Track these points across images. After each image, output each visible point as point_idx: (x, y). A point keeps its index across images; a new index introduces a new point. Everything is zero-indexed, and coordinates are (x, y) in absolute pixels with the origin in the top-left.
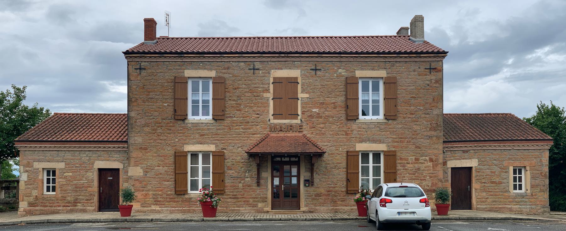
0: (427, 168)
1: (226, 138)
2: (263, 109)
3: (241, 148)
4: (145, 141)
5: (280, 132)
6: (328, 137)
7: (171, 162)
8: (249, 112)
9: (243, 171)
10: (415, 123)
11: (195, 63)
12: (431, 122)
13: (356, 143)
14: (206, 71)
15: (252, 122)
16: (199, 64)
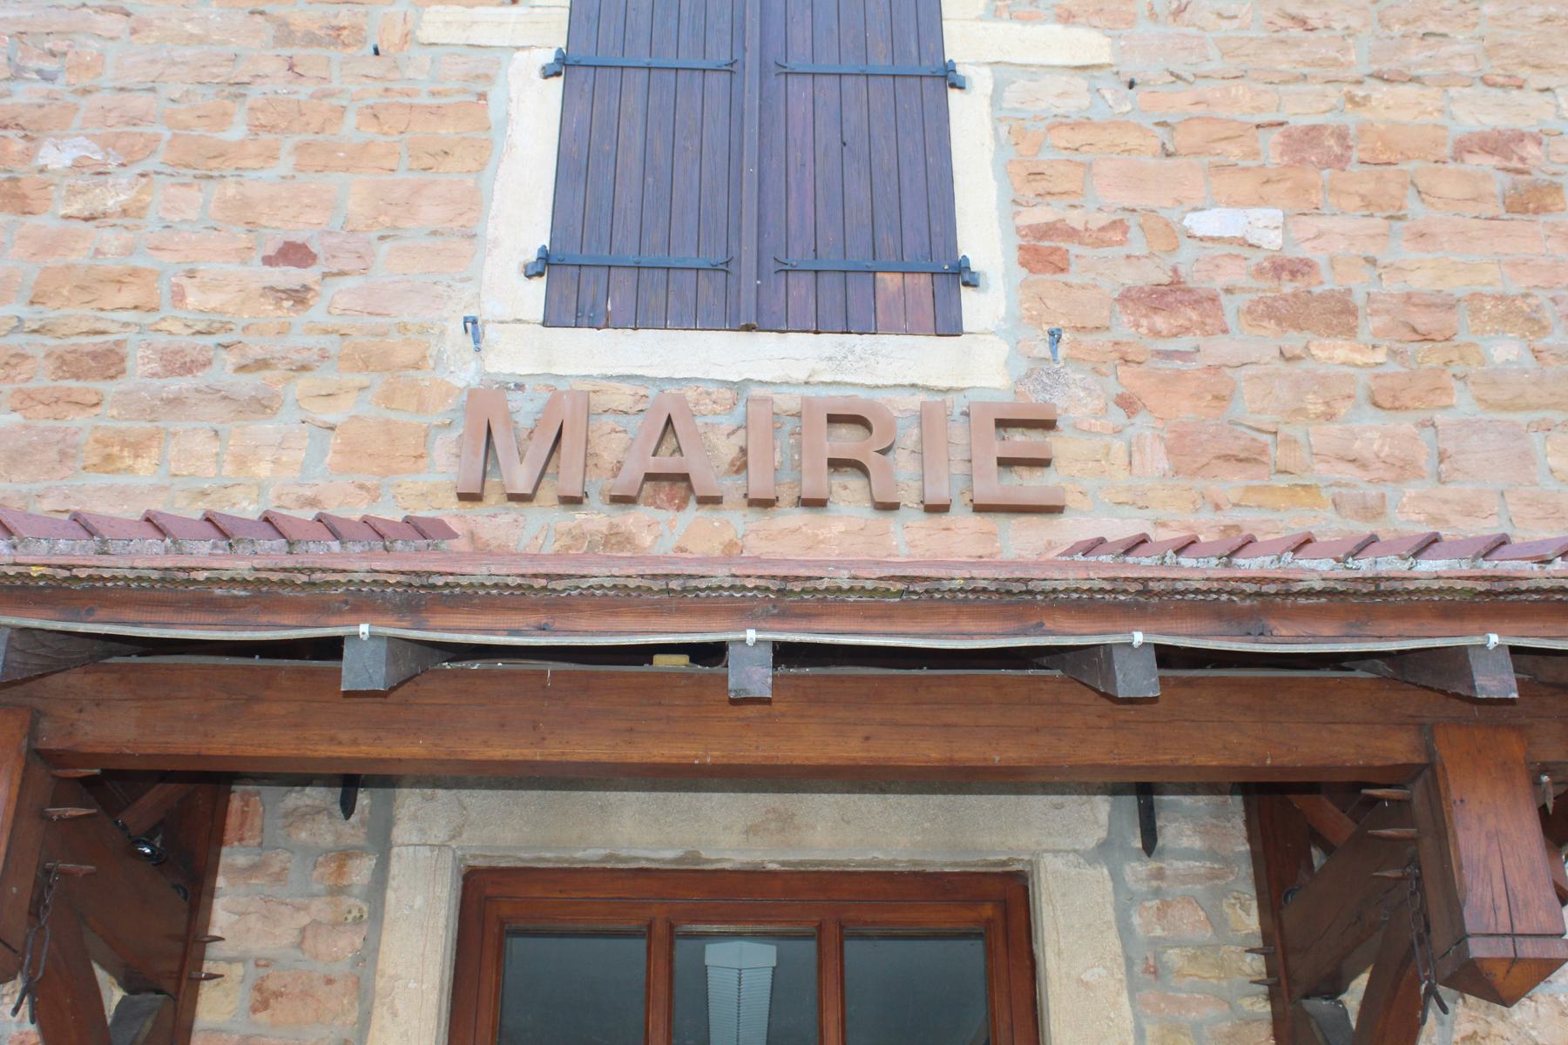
15: (179, 364)
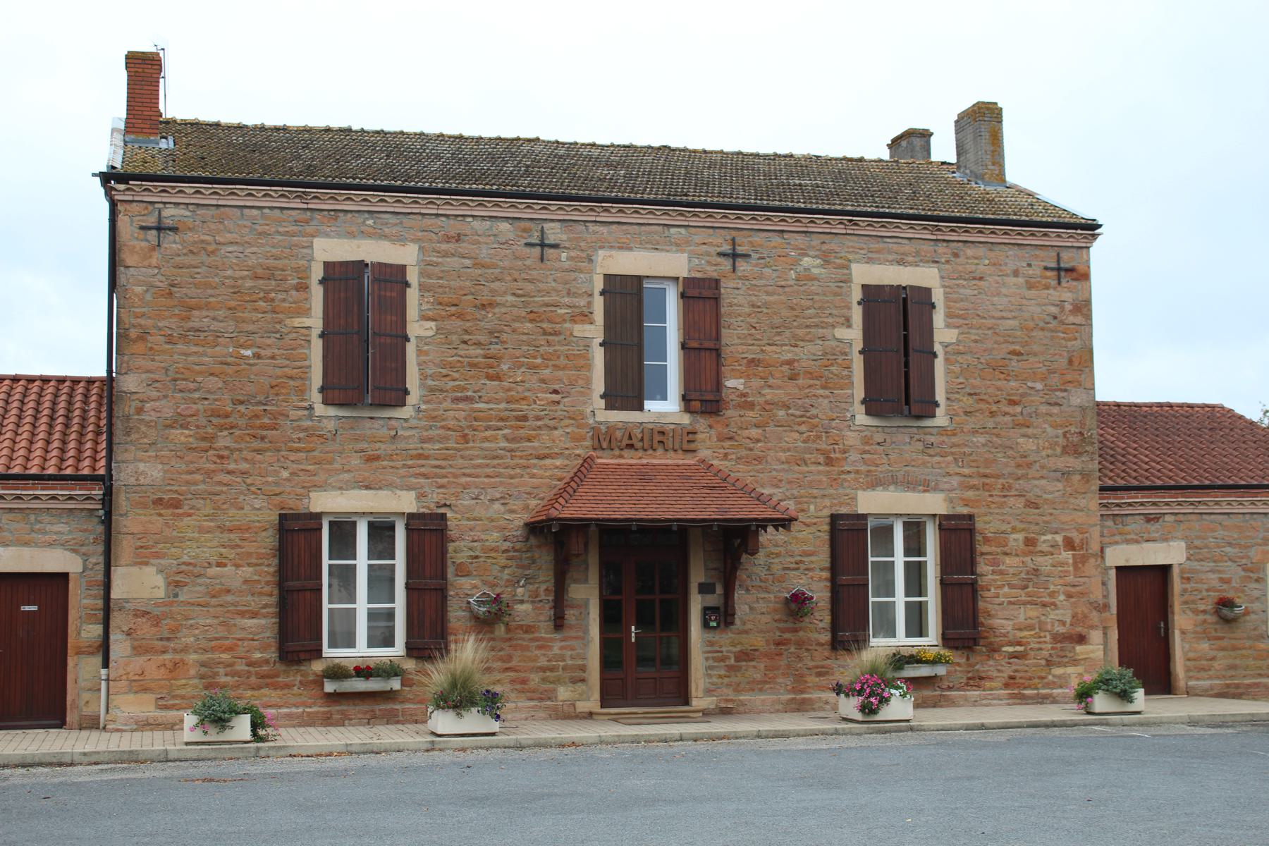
0: (1060, 569)
1: (450, 470)
2: (573, 375)
3: (503, 504)
4: (174, 476)
5: (626, 450)
6: (774, 469)
7: (264, 551)
8: (527, 385)
9: (508, 581)
10: (1024, 430)
11: (350, 215)
12: (1066, 429)
13: (857, 489)
14: (386, 244)
15: (538, 418)
16: (364, 221)
